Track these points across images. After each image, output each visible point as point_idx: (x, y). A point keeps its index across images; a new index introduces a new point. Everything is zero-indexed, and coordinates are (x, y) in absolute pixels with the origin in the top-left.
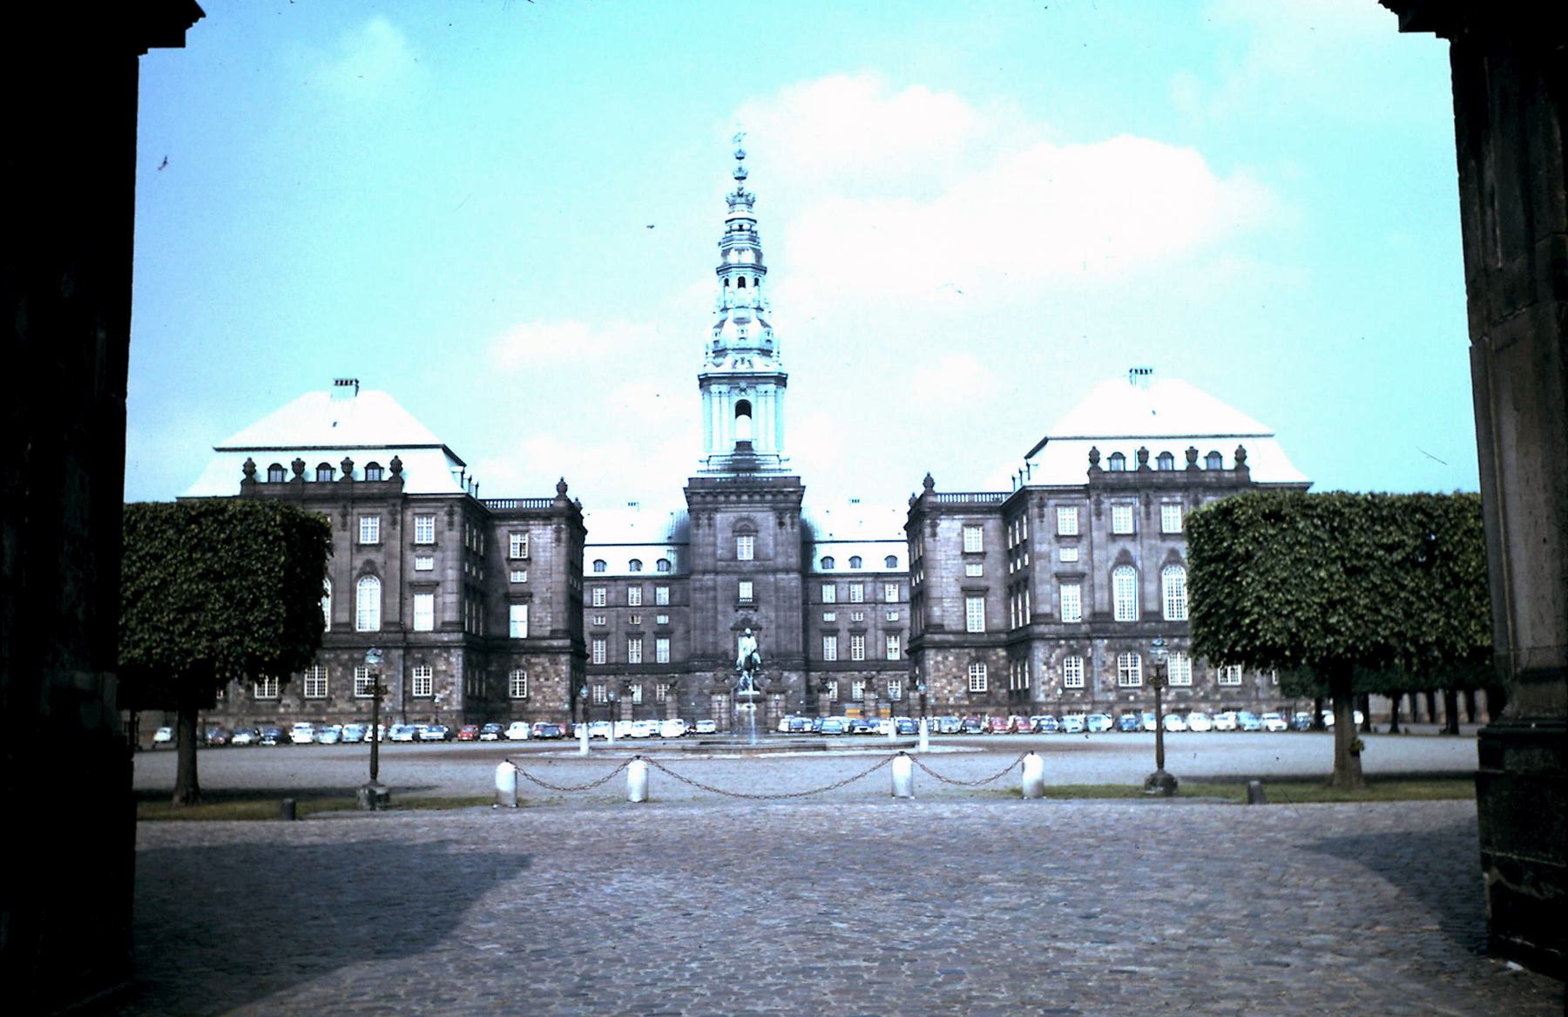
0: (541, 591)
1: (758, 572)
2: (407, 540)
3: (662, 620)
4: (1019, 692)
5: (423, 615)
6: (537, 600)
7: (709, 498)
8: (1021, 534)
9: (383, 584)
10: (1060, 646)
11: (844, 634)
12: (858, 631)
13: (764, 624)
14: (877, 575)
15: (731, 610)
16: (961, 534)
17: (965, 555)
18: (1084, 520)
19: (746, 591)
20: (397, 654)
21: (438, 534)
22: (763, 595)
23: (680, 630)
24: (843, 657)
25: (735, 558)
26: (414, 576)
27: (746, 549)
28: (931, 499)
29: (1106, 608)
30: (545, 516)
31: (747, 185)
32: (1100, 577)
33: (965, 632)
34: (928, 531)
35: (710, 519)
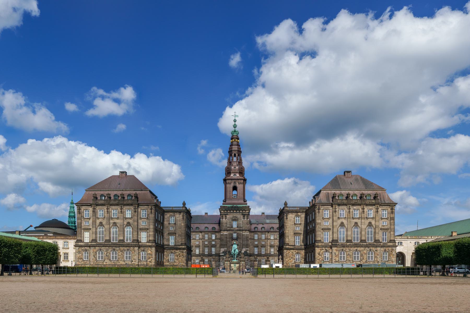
0: (178, 232)
1: (238, 230)
3: (213, 243)
5: (144, 237)
6: (177, 235)
7: (225, 211)
9: (132, 229)
11: (260, 247)
12: (263, 246)
15: (231, 240)
19: (235, 235)
20: (136, 248)
21: (148, 215)
22: (239, 237)
23: (218, 246)
24: (260, 253)
25: (232, 227)
26: (141, 227)
27: (235, 225)
28: (286, 208)
29: (336, 239)
30: (180, 212)
32: (335, 230)
33: (295, 245)
34: (285, 217)
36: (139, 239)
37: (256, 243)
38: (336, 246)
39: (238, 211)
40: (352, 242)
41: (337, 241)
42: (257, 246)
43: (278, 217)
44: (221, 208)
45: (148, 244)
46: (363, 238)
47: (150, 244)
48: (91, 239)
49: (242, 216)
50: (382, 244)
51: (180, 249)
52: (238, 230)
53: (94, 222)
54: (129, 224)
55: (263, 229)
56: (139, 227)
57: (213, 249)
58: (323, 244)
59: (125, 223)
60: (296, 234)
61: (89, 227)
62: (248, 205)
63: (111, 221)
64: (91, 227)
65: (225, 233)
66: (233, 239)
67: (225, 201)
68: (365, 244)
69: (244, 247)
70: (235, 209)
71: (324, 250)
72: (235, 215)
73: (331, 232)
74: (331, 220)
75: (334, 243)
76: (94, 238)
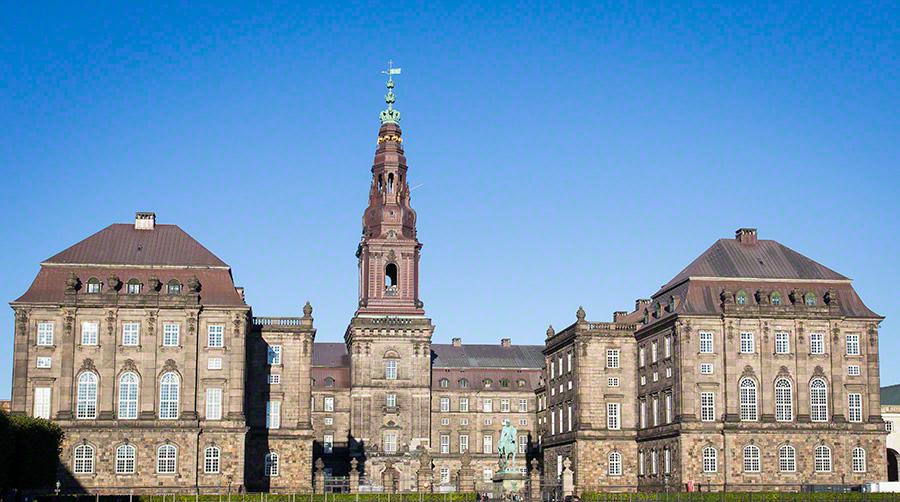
2: (201, 344)
3: (329, 422)
10: (700, 440)
13: (404, 426)
18: (720, 343)
19: (391, 401)
20: (192, 436)
22: (404, 405)
25: (384, 378)
28: (583, 327)
36: (200, 411)
38: (735, 429)
39: (401, 332)
40: (774, 421)
41: (736, 418)
45: (225, 424)
46: (803, 411)
47: (231, 424)
48: (55, 412)
49: (411, 347)
50: (850, 426)
51: (295, 438)
53: (68, 360)
54: (171, 365)
56: (200, 376)
59: (162, 363)
61: (50, 375)
63: (120, 357)
64: (57, 374)
65: (366, 393)
66: (386, 410)
67: (364, 303)
68: (809, 426)
69: (416, 433)
71: (704, 443)
72: (392, 343)
75: (730, 422)
76: (66, 407)
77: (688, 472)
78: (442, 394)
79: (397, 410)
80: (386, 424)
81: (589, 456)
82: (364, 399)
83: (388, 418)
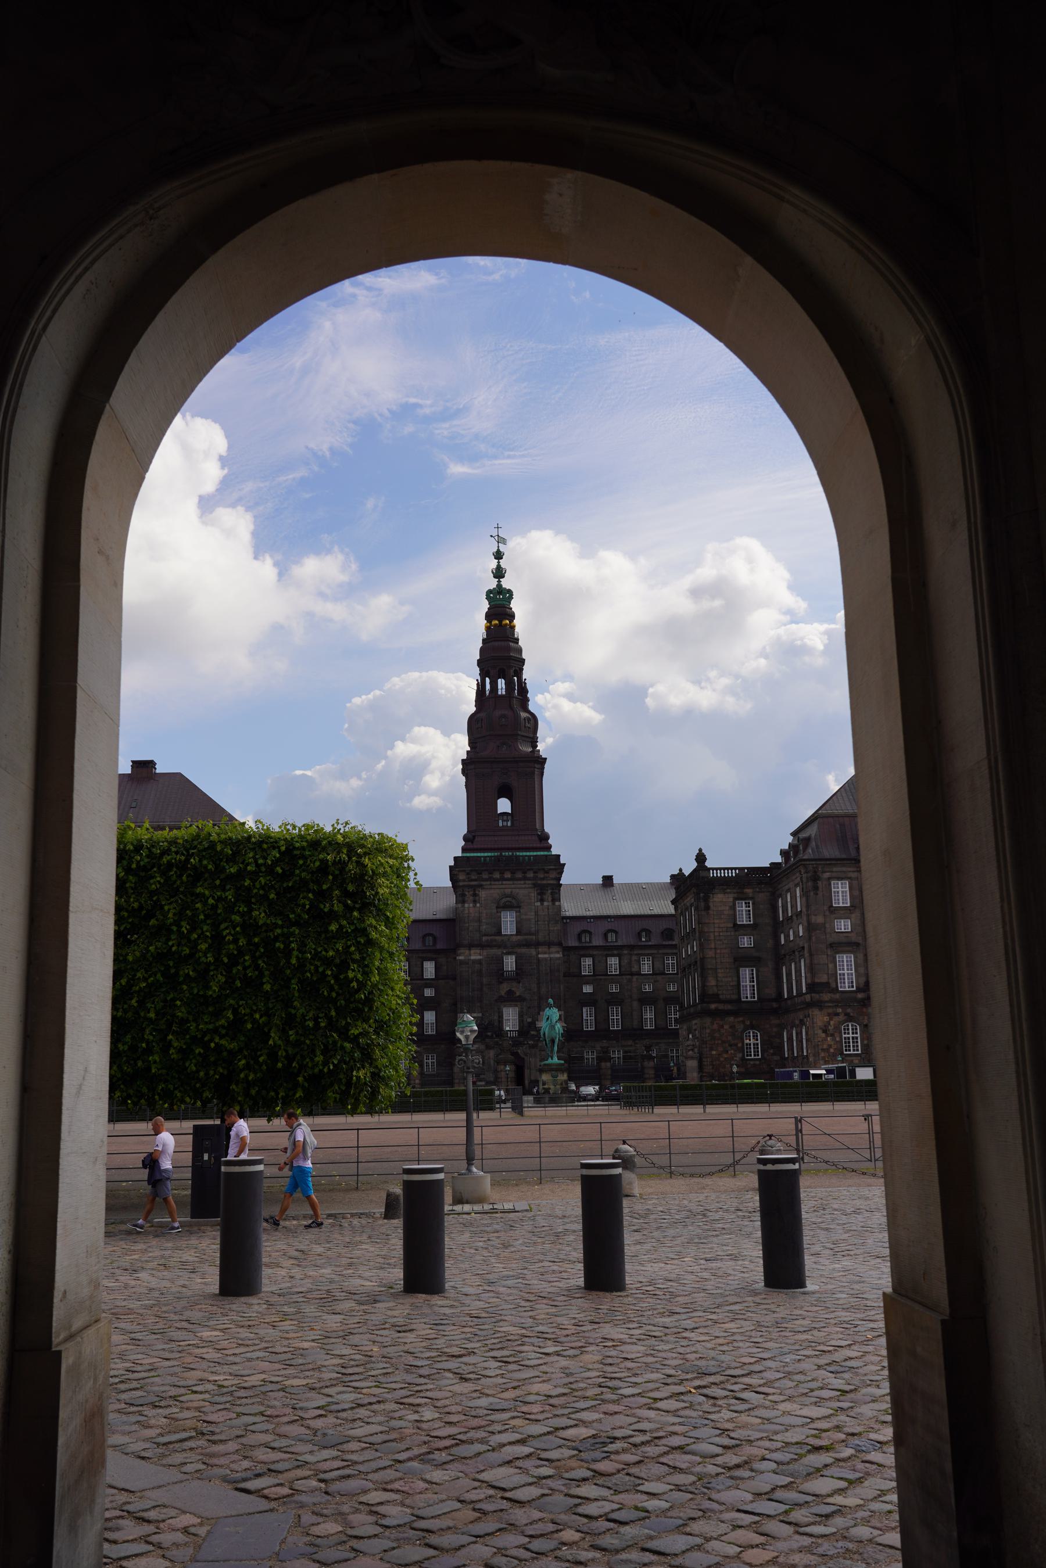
4: (794, 1058)
8: (794, 906)
10: (837, 1014)
12: (615, 1000)
14: (631, 947)
16: (733, 907)
17: (736, 927)
19: (510, 963)
25: (499, 933)
27: (509, 923)
28: (702, 874)
31: (506, 583)
35: (475, 895)
37: (588, 989)
39: (519, 875)
42: (589, 1001)
43: (673, 902)
44: (458, 869)
49: (534, 894)
52: (520, 945)
55: (611, 937)
57: (430, 1017)
58: (837, 996)
60: (742, 959)
62: (554, 851)
65: (475, 955)
70: (507, 867)
71: (842, 1017)
73: (861, 956)
74: (856, 915)
77: (822, 1054)
78: (582, 952)
79: (517, 974)
80: (503, 993)
81: (717, 1035)
82: (474, 961)
83: (504, 988)
